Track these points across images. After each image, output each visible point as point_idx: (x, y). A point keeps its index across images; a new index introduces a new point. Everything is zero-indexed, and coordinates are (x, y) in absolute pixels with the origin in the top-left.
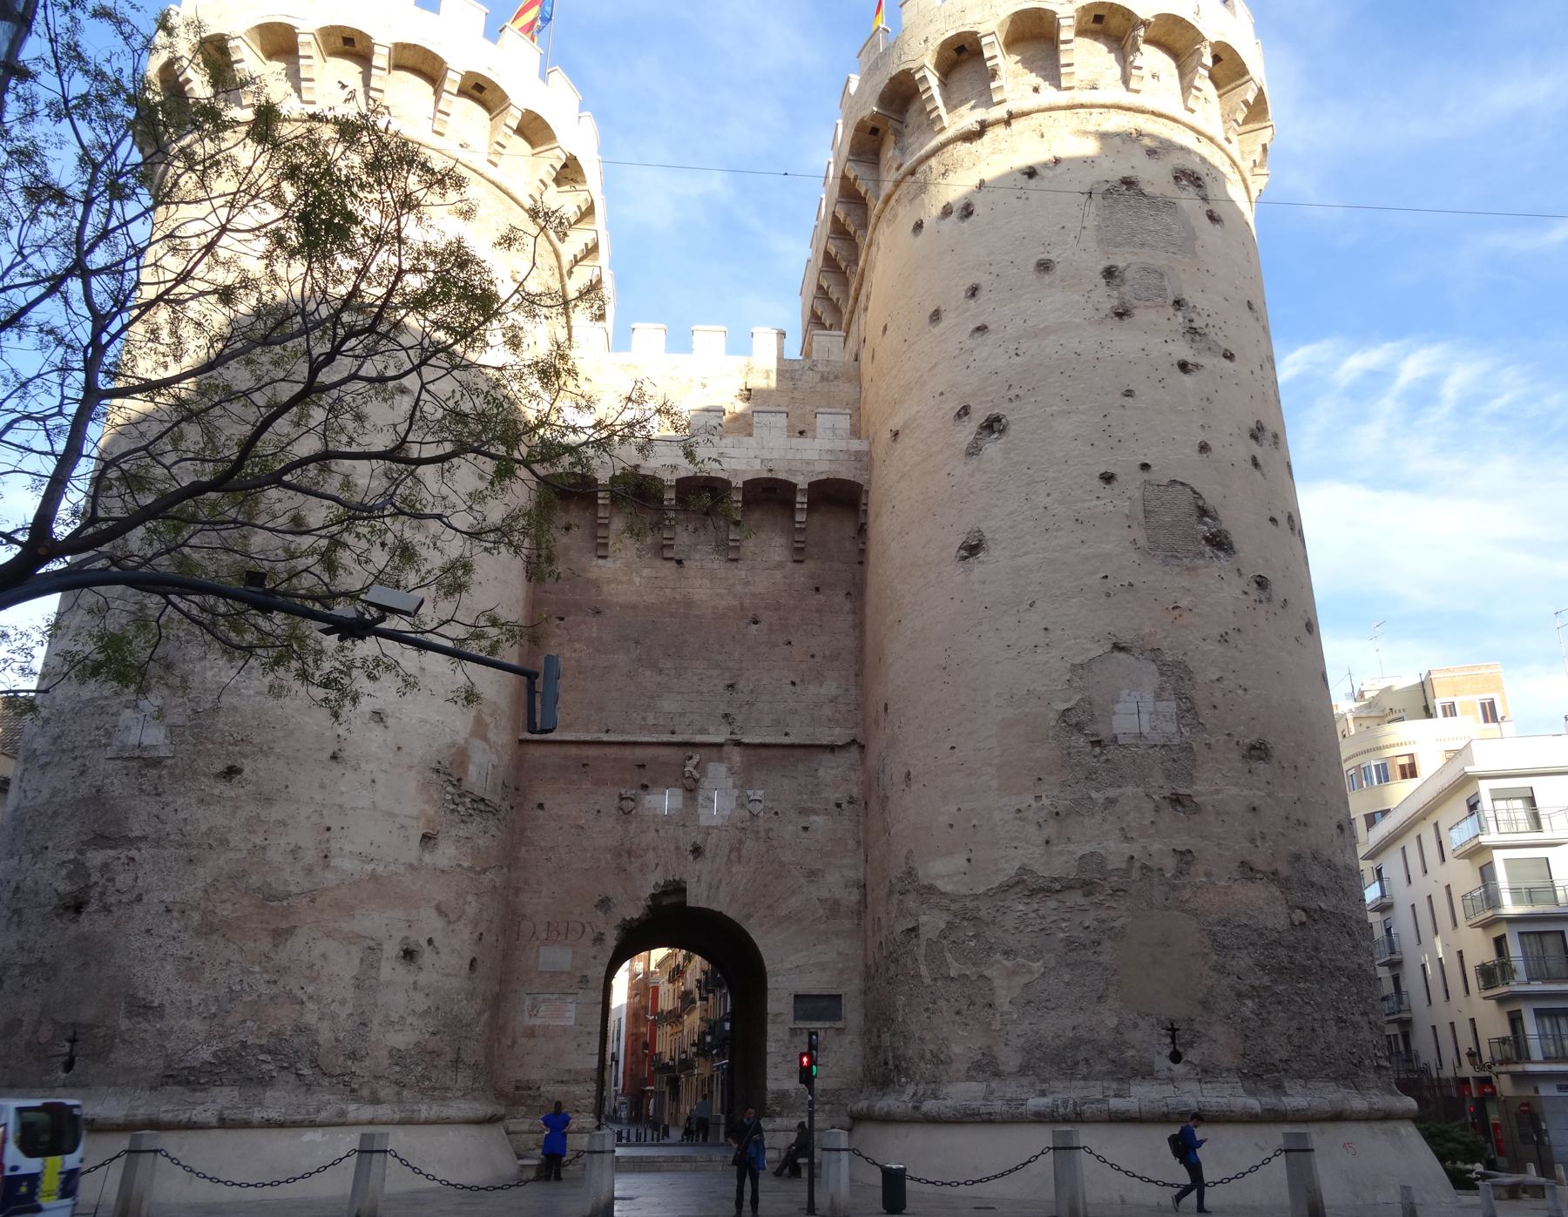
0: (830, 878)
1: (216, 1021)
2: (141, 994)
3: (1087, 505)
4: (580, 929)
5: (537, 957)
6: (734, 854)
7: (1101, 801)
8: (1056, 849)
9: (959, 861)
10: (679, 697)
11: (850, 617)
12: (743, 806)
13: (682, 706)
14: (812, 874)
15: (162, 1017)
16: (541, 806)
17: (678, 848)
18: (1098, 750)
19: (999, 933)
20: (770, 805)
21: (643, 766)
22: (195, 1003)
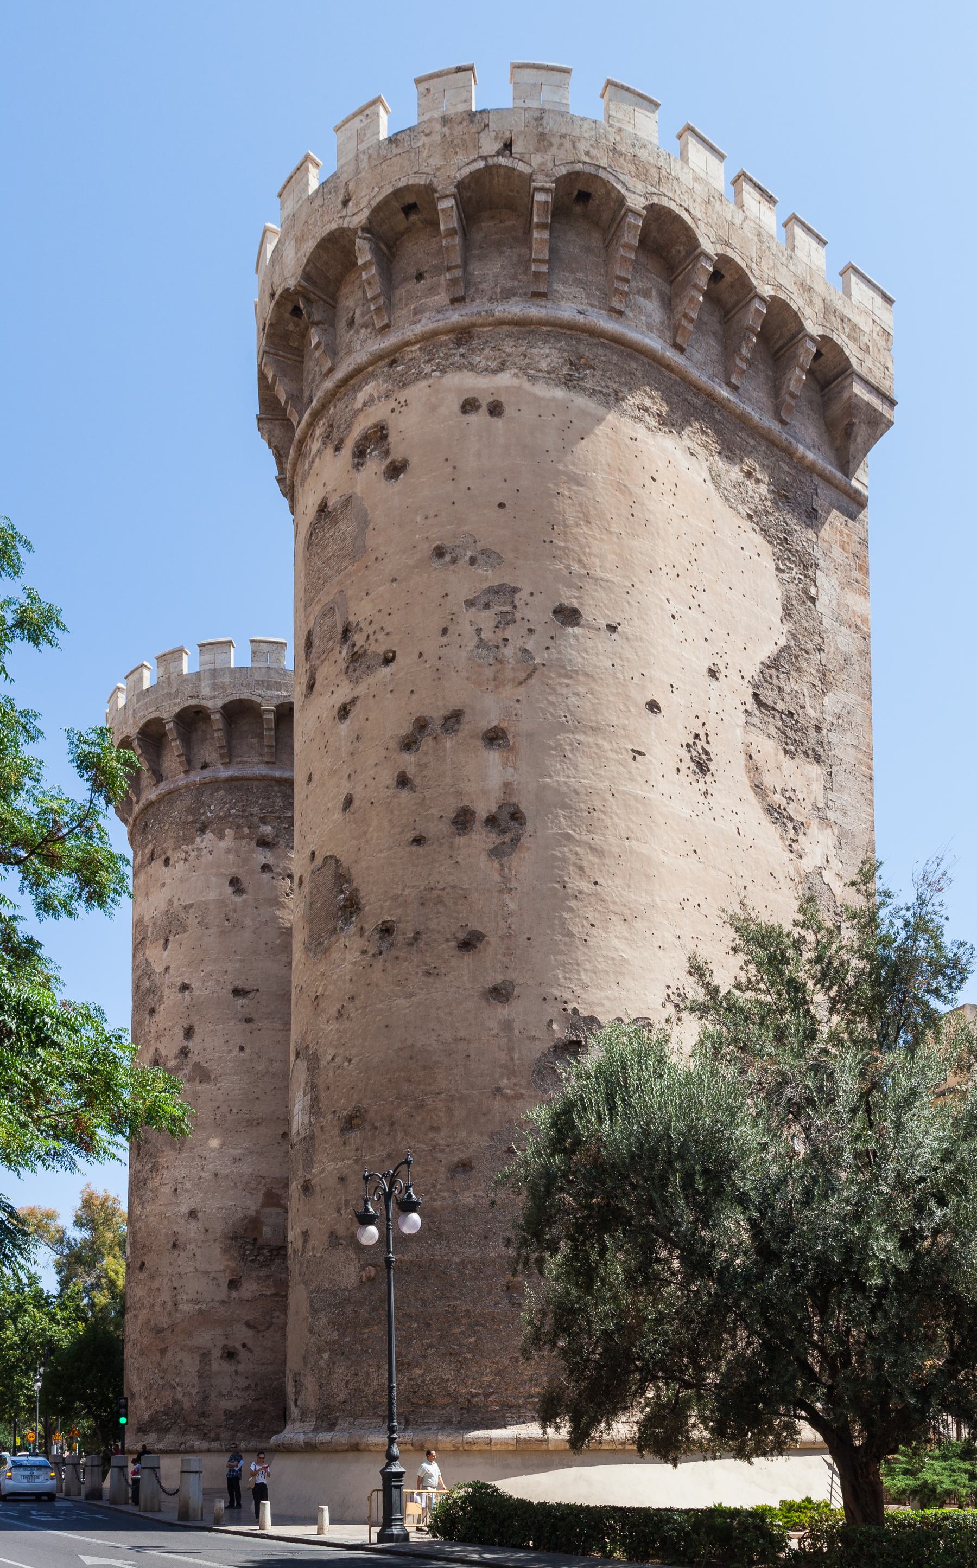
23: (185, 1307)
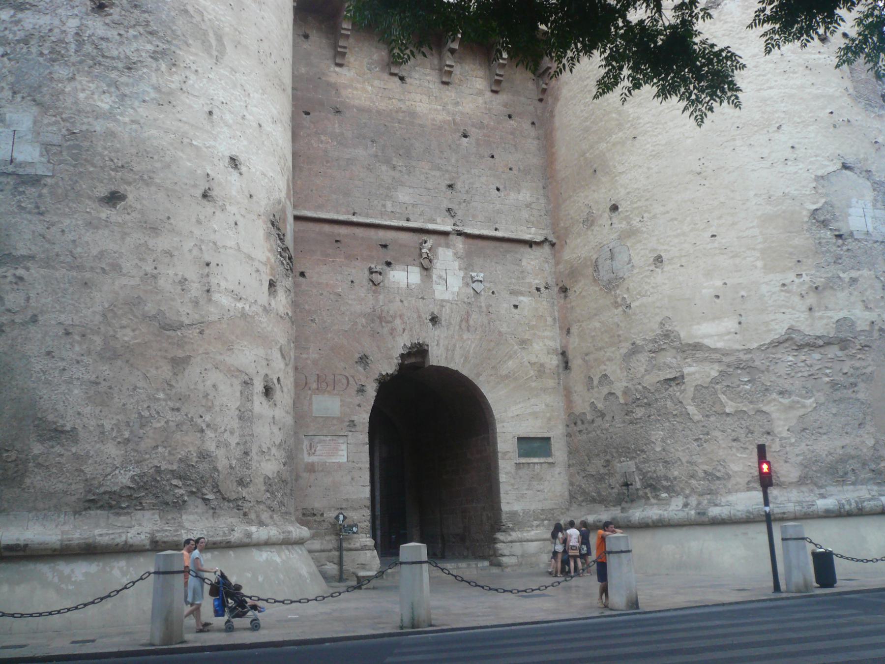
0: (534, 345)
1: (131, 446)
2: (51, 417)
3: (813, 56)
4: (344, 381)
5: (311, 404)
6: (464, 324)
7: (847, 280)
8: (817, 314)
9: (730, 324)
10: (411, 190)
11: (536, 142)
12: (468, 285)
13: (410, 200)
14: (523, 343)
15: (76, 441)
16: (302, 274)
17: (419, 317)
18: (840, 242)
19: (773, 378)
20: (488, 285)
21: (385, 246)
22: (108, 427)
23: (225, 301)
